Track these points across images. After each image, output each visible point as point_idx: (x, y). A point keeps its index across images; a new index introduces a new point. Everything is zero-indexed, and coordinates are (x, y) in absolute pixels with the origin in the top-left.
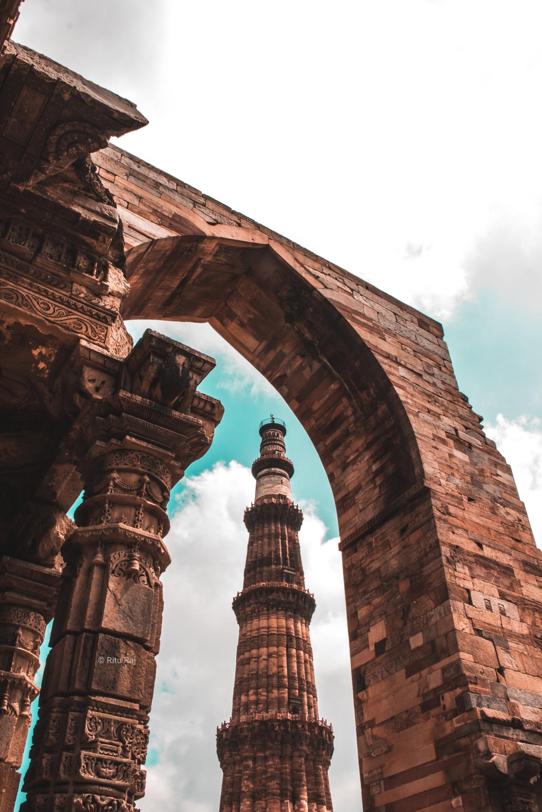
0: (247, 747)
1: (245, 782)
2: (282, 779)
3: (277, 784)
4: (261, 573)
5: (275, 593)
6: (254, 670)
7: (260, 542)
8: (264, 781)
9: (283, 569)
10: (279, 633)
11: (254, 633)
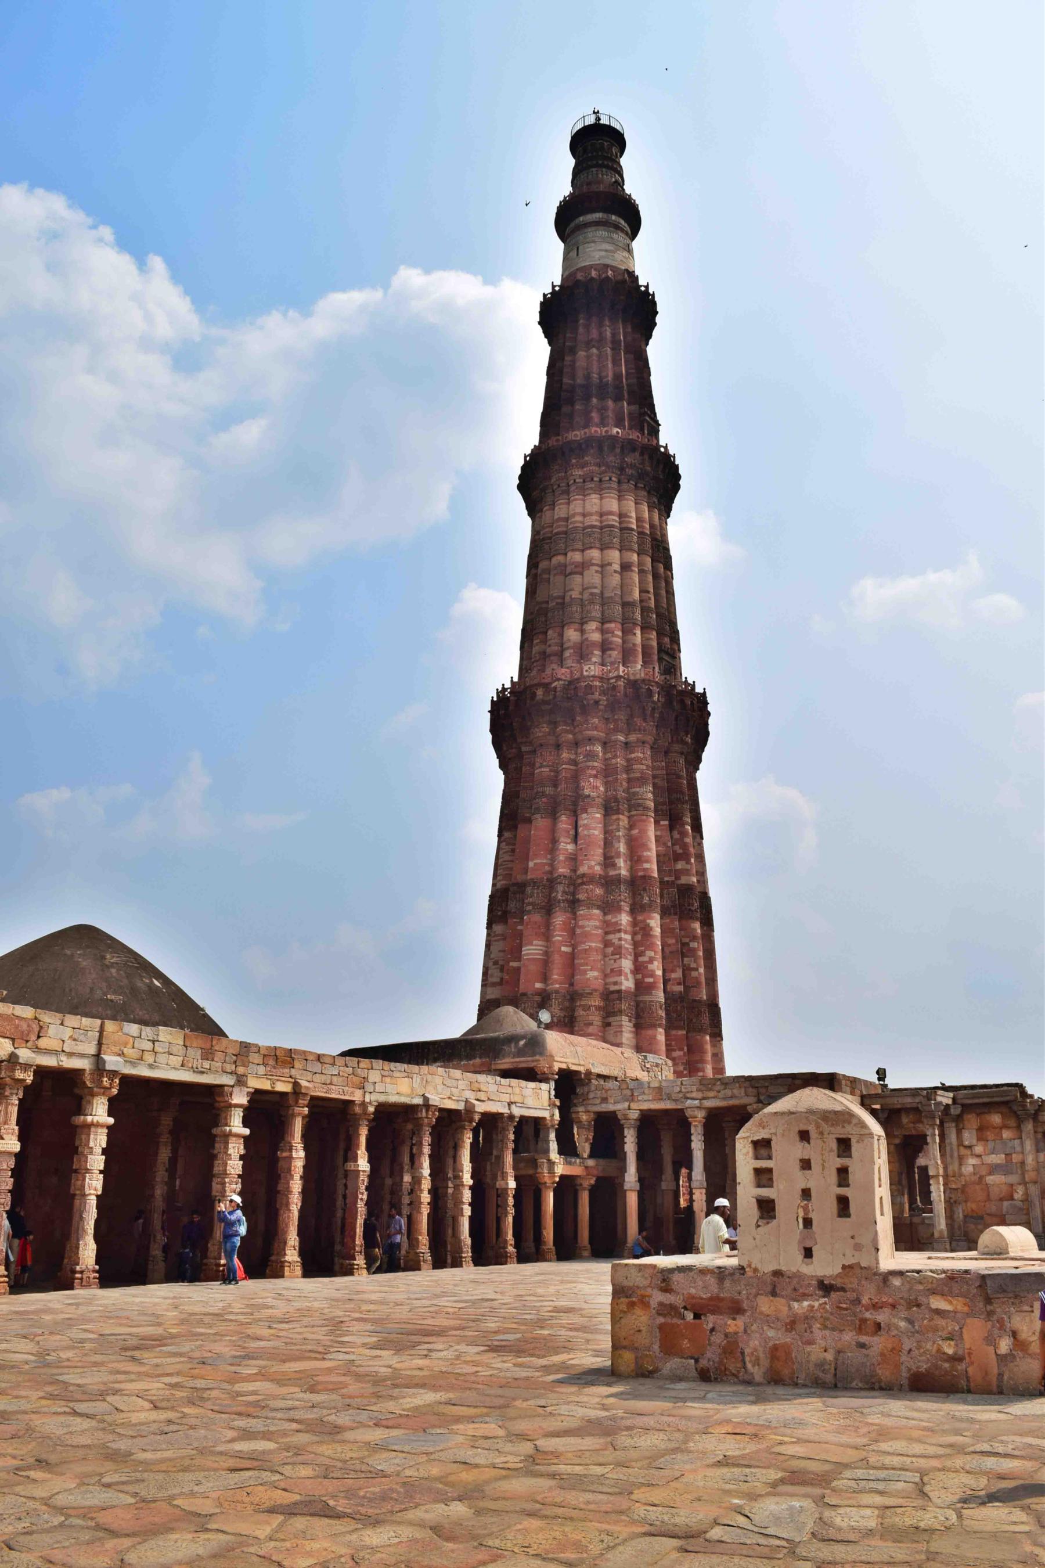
4: (602, 410)
5: (637, 454)
6: (596, 588)
7: (594, 351)
11: (594, 520)
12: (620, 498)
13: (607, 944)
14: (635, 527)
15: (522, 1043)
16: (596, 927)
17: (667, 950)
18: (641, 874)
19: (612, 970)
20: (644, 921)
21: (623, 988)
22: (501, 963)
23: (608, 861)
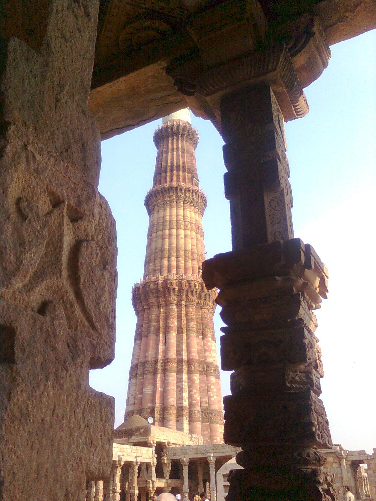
1: (172, 320)
8: (185, 322)
9: (193, 177)
10: (191, 222)
12: (184, 209)
13: (178, 387)
14: (189, 221)
15: (142, 431)
16: (173, 380)
17: (201, 389)
22: (134, 395)
23: (179, 353)
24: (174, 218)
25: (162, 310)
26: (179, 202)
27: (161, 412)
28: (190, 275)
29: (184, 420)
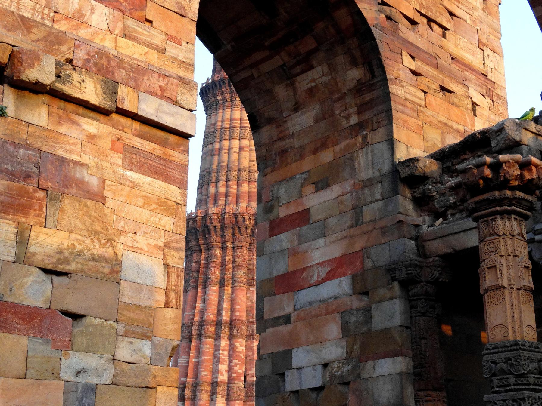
0: (215, 237)
1: (212, 269)
2: (249, 269)
3: (243, 273)
6: (224, 162)
8: (231, 270)
13: (215, 356)
16: (209, 349)
17: (248, 358)
18: (234, 318)
19: (216, 371)
20: (234, 344)
21: (219, 380)
24: (227, 124)
25: (203, 256)
26: (234, 99)
27: (193, 389)
28: (243, 204)
29: (217, 399)
